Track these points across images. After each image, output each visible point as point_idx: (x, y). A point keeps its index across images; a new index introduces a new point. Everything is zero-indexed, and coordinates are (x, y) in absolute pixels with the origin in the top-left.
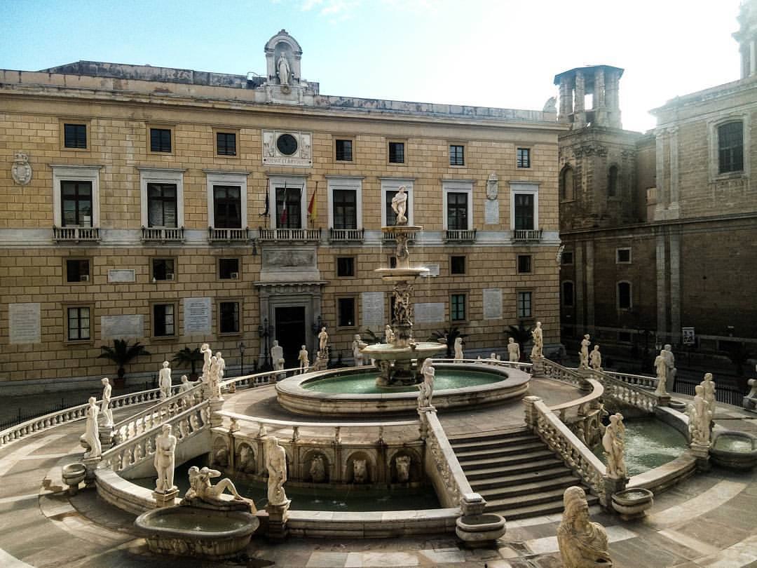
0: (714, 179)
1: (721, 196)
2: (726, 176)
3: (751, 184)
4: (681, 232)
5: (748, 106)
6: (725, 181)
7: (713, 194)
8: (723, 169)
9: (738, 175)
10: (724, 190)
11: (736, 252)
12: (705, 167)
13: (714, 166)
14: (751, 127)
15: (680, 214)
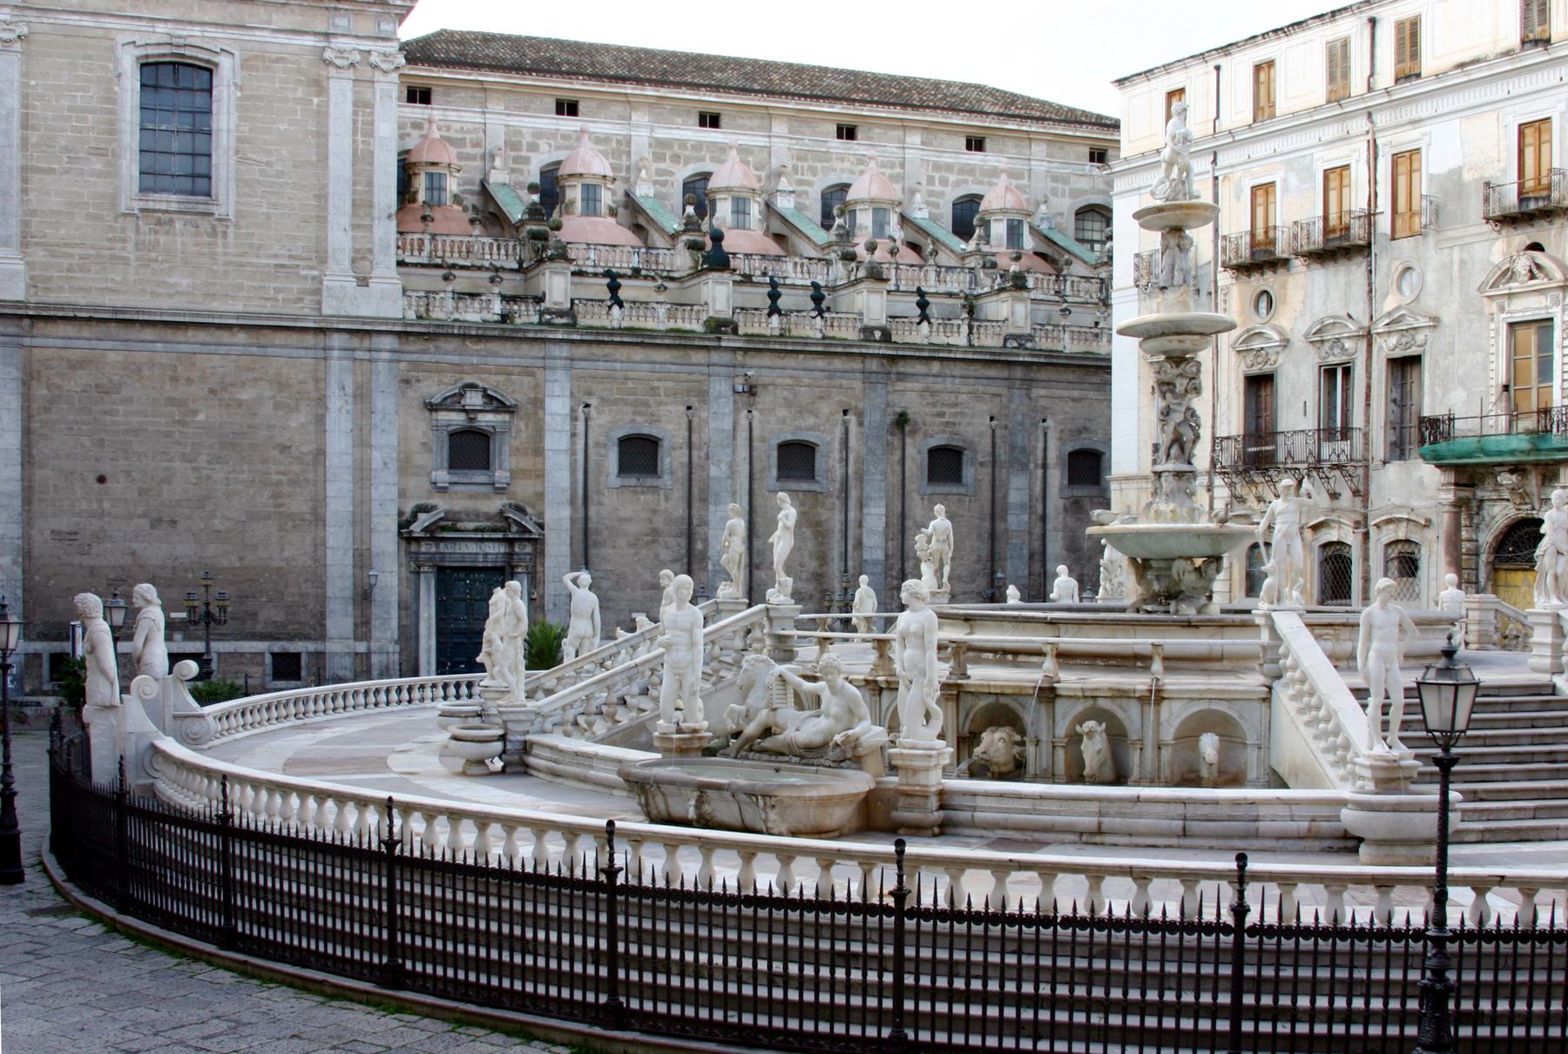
0: (137, 205)
1: (153, 255)
2: (167, 201)
3: (237, 235)
4: (27, 341)
5: (236, 34)
6: (167, 216)
7: (130, 246)
8: (151, 179)
9: (201, 208)
10: (162, 239)
11: (195, 412)
12: (108, 164)
13: (130, 166)
14: (241, 89)
15: (28, 287)
